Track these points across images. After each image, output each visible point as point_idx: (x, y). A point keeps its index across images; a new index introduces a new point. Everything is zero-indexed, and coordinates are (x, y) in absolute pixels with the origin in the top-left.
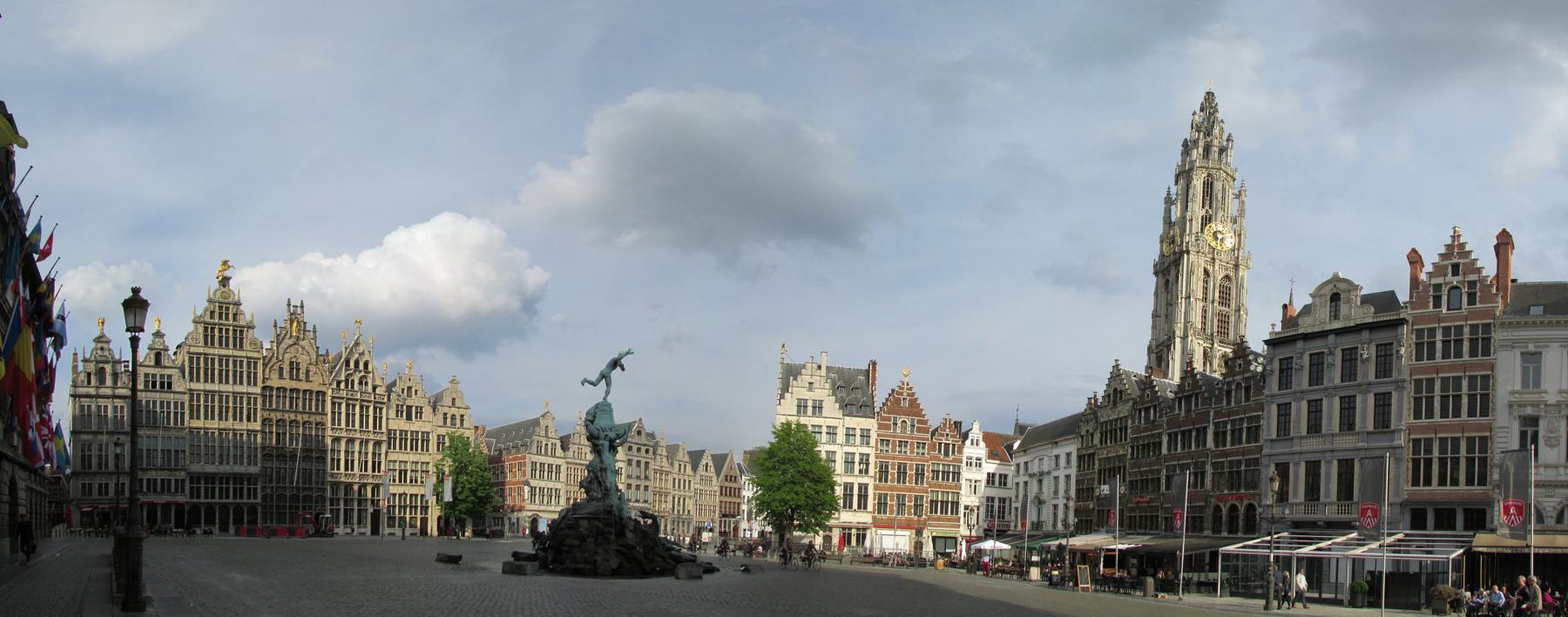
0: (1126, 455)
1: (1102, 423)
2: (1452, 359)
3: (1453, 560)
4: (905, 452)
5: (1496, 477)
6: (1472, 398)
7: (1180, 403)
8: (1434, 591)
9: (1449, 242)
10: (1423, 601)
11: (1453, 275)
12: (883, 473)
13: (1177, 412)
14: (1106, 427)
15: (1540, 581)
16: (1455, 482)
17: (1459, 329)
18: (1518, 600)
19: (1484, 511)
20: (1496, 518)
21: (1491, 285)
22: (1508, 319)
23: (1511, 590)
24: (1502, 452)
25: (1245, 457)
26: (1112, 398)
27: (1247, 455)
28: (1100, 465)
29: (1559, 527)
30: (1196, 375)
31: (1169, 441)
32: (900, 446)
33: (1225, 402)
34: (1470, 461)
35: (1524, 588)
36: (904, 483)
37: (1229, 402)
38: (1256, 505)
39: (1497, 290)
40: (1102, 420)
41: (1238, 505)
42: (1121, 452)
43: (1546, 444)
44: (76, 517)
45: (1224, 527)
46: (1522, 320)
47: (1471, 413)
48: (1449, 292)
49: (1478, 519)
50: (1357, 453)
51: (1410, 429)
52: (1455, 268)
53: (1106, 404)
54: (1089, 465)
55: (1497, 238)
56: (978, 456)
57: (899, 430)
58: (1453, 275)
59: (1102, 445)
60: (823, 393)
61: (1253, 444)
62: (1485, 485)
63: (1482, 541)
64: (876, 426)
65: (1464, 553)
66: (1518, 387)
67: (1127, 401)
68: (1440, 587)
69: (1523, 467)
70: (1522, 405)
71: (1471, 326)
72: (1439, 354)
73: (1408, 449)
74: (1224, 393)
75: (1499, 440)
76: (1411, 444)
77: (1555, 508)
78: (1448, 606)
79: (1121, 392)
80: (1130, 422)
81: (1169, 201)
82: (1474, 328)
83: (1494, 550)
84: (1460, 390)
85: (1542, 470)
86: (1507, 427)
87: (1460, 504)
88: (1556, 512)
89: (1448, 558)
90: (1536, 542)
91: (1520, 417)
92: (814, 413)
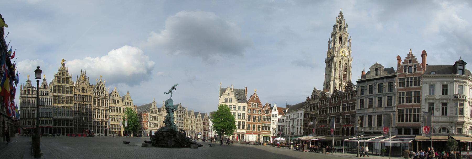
0: (317, 113)
1: (311, 105)
2: (409, 87)
3: (410, 143)
4: (255, 113)
5: (422, 120)
6: (415, 97)
8: (404, 152)
9: (409, 54)
10: (401, 154)
11: (410, 63)
12: (249, 119)
14: (312, 106)
15: (434, 149)
16: (410, 121)
17: (411, 78)
18: (428, 154)
19: (418, 129)
20: (422, 131)
22: (425, 75)
23: (426, 152)
24: (424, 113)
26: (313, 98)
28: (310, 116)
29: (440, 134)
30: (337, 91)
32: (254, 111)
33: (345, 99)
34: (415, 115)
35: (430, 151)
36: (255, 121)
37: (346, 99)
39: (422, 67)
40: (311, 104)
42: (316, 113)
44: (21, 131)
45: (345, 134)
46: (429, 76)
47: (415, 102)
48: (408, 68)
49: (417, 132)
51: (398, 106)
52: (410, 61)
53: (312, 99)
56: (276, 114)
57: (253, 107)
58: (410, 63)
59: (311, 111)
60: (232, 96)
62: (419, 122)
63: (418, 138)
64: (247, 105)
65: (413, 141)
66: (428, 94)
67: (318, 98)
68: (406, 150)
69: (429, 117)
71: (415, 77)
72: (406, 85)
75: (423, 109)
76: (398, 111)
77: (438, 129)
78: (408, 156)
79: (316, 96)
80: (319, 104)
81: (330, 42)
83: (421, 140)
84: (412, 95)
85: (435, 118)
86: (425, 106)
87: (411, 127)
88: (439, 129)
89: (408, 143)
90: (433, 138)
91: (428, 103)
92: (229, 102)
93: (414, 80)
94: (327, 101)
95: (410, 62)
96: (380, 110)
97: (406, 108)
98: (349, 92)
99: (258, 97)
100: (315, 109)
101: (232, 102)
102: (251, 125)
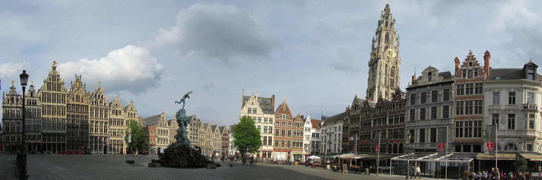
0: (359, 127)
1: (351, 116)
3: (470, 162)
4: (284, 126)
5: (484, 134)
6: (476, 108)
7: (377, 109)
8: (463, 173)
9: (468, 55)
10: (459, 176)
11: (470, 66)
12: (277, 133)
13: (376, 112)
14: (352, 118)
15: (499, 169)
16: (470, 136)
17: (472, 84)
18: (492, 176)
19: (480, 146)
20: (484, 148)
21: (483, 70)
22: (488, 81)
23: (489, 173)
24: (486, 126)
25: (399, 128)
26: (354, 107)
27: (400, 127)
28: (350, 130)
29: (506, 151)
30: (383, 100)
31: (374, 122)
32: (283, 124)
33: (392, 109)
34: (476, 129)
35: (494, 172)
36: (284, 136)
37: (394, 109)
38: (403, 144)
39: (485, 71)
40: (351, 115)
41: (397, 143)
42: (358, 126)
43: (501, 123)
44: (4, 148)
45: (392, 151)
46: (493, 81)
47: (476, 113)
48: (468, 72)
49: (478, 148)
50: (437, 126)
51: (455, 118)
52: (471, 64)
53: (352, 110)
54: (347, 130)
55: (485, 54)
57: (282, 119)
58: (470, 66)
59: (351, 123)
60: (257, 106)
61: (402, 123)
62: (481, 137)
63: (480, 156)
64: (275, 117)
65: (473, 160)
66: (492, 104)
67: (359, 109)
68: (465, 171)
69: (493, 131)
70: (493, 110)
71: (476, 83)
72: (465, 93)
73: (455, 125)
74: (392, 106)
75: (485, 122)
76: (455, 123)
77: (504, 145)
78: (468, 178)
79: (357, 106)
80: (360, 116)
81: (374, 41)
82: (477, 84)
83: (484, 159)
84: (472, 105)
85: (500, 132)
86: (488, 118)
87: (472, 143)
88: (504, 146)
89: (468, 162)
90: (498, 156)
91: (492, 114)
92: (254, 113)
93: (475, 87)
94: (371, 111)
95: (470, 66)
96: (434, 122)
97: (465, 120)
98: (397, 101)
99: (288, 107)
100: (357, 121)
101: (257, 113)
102: (280, 141)
